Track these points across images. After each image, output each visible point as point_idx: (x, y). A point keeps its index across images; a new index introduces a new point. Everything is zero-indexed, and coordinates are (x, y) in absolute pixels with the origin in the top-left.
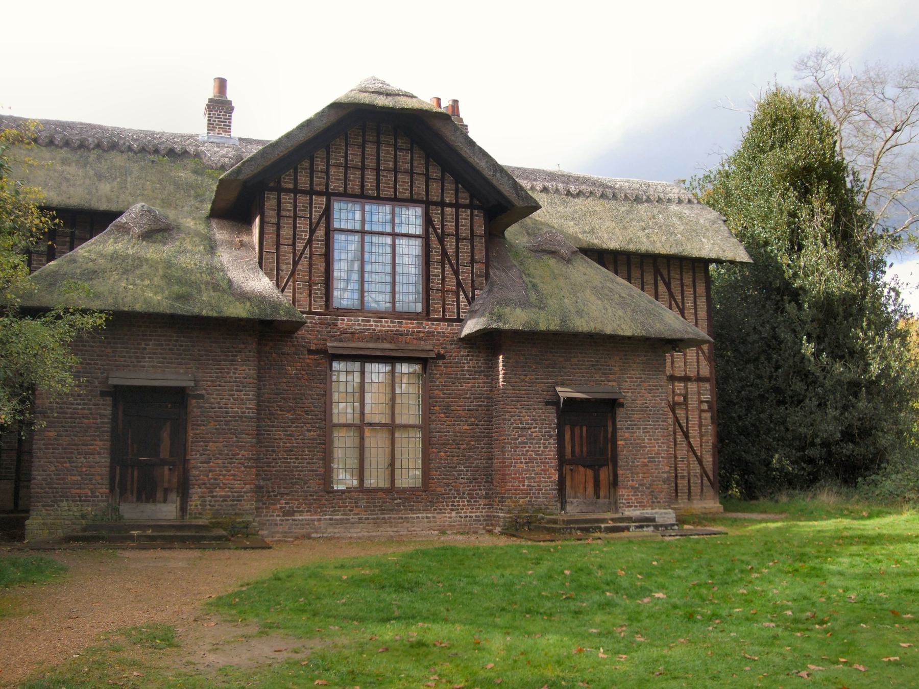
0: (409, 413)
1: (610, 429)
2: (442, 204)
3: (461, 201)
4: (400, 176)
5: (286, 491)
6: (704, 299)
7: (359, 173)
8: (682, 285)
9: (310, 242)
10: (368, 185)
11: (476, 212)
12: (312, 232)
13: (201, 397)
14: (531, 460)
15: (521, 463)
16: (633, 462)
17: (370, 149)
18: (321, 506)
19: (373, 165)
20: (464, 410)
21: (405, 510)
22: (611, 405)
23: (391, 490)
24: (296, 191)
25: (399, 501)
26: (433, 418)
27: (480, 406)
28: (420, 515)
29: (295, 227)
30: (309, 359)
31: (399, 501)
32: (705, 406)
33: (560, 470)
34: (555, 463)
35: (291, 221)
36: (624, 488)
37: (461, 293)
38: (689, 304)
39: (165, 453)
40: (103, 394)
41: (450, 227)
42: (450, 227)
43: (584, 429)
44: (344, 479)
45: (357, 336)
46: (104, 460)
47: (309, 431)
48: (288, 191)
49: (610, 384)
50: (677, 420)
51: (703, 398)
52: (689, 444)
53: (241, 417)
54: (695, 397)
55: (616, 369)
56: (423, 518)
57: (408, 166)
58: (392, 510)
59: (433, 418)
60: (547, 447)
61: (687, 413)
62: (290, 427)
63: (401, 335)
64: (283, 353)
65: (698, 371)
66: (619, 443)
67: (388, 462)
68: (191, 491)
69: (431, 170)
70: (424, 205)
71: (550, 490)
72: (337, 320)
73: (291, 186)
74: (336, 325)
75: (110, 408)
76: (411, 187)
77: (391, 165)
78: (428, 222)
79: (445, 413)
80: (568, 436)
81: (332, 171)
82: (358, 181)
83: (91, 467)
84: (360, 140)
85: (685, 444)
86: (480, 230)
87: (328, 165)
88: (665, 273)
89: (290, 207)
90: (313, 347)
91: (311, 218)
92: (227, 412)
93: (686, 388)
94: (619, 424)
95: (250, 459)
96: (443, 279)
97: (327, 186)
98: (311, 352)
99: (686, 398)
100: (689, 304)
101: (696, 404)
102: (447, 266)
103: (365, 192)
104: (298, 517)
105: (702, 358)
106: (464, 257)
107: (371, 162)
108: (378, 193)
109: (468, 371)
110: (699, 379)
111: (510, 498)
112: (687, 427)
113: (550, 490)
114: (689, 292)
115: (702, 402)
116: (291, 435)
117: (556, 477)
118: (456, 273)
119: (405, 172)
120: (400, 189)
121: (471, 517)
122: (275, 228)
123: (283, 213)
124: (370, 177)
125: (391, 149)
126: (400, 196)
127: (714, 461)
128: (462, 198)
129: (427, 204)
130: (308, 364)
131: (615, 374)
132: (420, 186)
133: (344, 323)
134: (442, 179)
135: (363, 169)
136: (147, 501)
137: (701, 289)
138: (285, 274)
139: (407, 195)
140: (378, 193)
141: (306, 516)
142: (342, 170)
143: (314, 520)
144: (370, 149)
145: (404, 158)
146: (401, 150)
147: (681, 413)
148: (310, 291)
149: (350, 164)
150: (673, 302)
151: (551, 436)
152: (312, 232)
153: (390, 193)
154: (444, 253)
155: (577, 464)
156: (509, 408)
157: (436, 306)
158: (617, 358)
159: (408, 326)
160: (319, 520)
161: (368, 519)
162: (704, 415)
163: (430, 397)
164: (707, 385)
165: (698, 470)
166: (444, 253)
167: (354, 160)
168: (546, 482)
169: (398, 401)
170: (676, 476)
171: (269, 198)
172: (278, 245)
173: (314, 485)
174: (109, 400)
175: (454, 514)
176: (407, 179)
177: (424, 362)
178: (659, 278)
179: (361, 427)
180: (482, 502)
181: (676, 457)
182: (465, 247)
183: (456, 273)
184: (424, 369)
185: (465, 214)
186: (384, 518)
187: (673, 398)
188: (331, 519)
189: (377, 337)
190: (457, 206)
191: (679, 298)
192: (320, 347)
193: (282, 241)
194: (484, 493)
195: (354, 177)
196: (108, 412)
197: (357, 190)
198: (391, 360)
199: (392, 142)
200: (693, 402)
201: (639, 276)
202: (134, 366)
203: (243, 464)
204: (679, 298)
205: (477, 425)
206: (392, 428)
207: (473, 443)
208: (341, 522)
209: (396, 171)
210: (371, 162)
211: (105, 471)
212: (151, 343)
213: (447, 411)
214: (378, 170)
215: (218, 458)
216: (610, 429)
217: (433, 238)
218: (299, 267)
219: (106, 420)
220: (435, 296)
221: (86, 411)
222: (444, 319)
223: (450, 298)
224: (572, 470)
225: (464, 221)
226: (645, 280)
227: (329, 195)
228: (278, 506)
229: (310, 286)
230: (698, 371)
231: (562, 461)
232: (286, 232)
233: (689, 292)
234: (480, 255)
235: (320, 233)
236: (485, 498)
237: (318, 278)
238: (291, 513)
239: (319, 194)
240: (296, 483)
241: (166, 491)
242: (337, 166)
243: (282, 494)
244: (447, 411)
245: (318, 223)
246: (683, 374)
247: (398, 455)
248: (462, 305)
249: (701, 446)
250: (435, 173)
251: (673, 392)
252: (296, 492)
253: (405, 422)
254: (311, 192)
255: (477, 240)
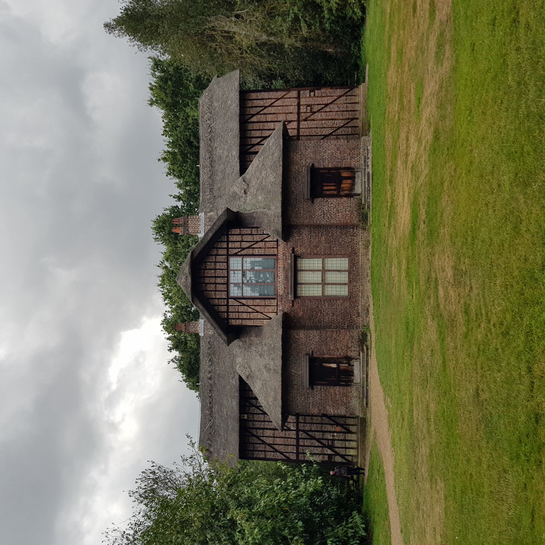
0: (317, 263)
1: (324, 171)
2: (228, 248)
3: (226, 240)
4: (217, 268)
5: (349, 315)
6: (259, 93)
7: (217, 285)
8: (252, 107)
9: (248, 306)
10: (222, 281)
11: (230, 233)
12: (244, 305)
13: (312, 351)
14: (338, 210)
15: (338, 215)
16: (339, 159)
17: (207, 280)
18: (356, 301)
19: (213, 279)
20: (316, 239)
21: (358, 265)
22: (314, 171)
23: (350, 272)
24: (228, 312)
25: (354, 268)
26: (319, 253)
27: (314, 231)
28: (360, 259)
29: (242, 312)
30: (296, 306)
31: (354, 268)
32: (312, 94)
33: (341, 196)
34: (339, 199)
35: (240, 314)
36: (351, 164)
37: (265, 240)
38: (261, 103)
39: (334, 366)
40: (312, 389)
41: (237, 245)
42: (237, 245)
43: (324, 184)
44: (344, 291)
45: (286, 286)
46: (337, 388)
47: (325, 306)
48: (228, 315)
49: (303, 170)
50: (318, 111)
51: (308, 95)
52: (331, 103)
53: (320, 336)
54: (308, 99)
55: (296, 167)
56: (361, 258)
57: (213, 264)
58: (358, 271)
59: (319, 253)
60: (332, 203)
61: (316, 105)
62: (324, 314)
63: (285, 267)
64: (294, 317)
65: (295, 98)
66: (330, 166)
67: (338, 273)
68: (349, 356)
69: (213, 254)
70: (229, 257)
71: (351, 201)
72: (279, 295)
73: (226, 314)
74: (281, 296)
75: (318, 386)
76: (221, 262)
77: (213, 271)
78: (236, 255)
79: (317, 248)
80: (328, 193)
81: (218, 297)
82: (221, 286)
83: (340, 393)
84: (204, 285)
85: (331, 106)
86: (237, 231)
87: (216, 299)
88: (247, 117)
89: (234, 314)
90: (291, 305)
91: (238, 306)
92: (318, 342)
93: (303, 105)
94: (322, 167)
95: (337, 333)
96: (260, 248)
97: (224, 299)
98: (293, 306)
99: (308, 106)
100: (261, 103)
101: (311, 99)
102: (254, 246)
103: (226, 283)
104: (360, 311)
105: (287, 96)
106: (250, 238)
107: (213, 280)
108: (226, 277)
109: (299, 237)
110: (299, 97)
111: (354, 220)
112: (323, 104)
113: (351, 201)
114: (256, 103)
115: (310, 95)
116: (327, 314)
117: (345, 199)
118: (257, 242)
119: (215, 265)
120: (223, 267)
121: (362, 236)
122: (243, 320)
123: (237, 317)
124: (219, 280)
125: (206, 271)
126: (226, 267)
127: (339, 89)
128: (224, 239)
129: (228, 255)
130: (298, 307)
131: (299, 168)
132: (219, 258)
133: (281, 292)
134: (217, 248)
135: (216, 284)
136: (353, 372)
137: (254, 96)
138: (261, 316)
139: (225, 264)
140: (226, 277)
141: (360, 307)
142: (217, 293)
143: (361, 305)
144: (207, 280)
145: (210, 265)
146: (206, 267)
147: (316, 108)
148: (268, 306)
149: (214, 289)
150: (261, 113)
151: (327, 201)
152: (244, 305)
153: (225, 271)
154: (249, 248)
155: (340, 188)
156: (315, 221)
157: (271, 251)
158: (292, 167)
159: (281, 264)
160: (361, 302)
161: (361, 282)
162: (316, 95)
163: (311, 254)
164: (302, 92)
165: (344, 98)
166: (249, 248)
167: (213, 286)
168: (347, 203)
169: (312, 268)
170: (347, 111)
171: (231, 323)
172: (250, 319)
173: (347, 304)
174: (315, 387)
175: (360, 244)
176: (218, 264)
177: (296, 257)
178: (250, 121)
179: (324, 283)
180: (355, 231)
181: (337, 111)
182: (246, 238)
183: (257, 242)
184: (299, 257)
185: (231, 238)
186: (361, 275)
187: (308, 113)
188: (361, 297)
189: (286, 277)
190: (228, 242)
191: (259, 109)
192: (291, 302)
193: (248, 317)
194: (351, 230)
195: (220, 287)
196: (319, 387)
197: (225, 286)
198: (296, 271)
199: (203, 271)
200: (310, 101)
201: (249, 132)
202: (301, 377)
203: (338, 335)
204: (259, 109)
205: (322, 233)
206: (324, 271)
207: (330, 235)
208: (362, 293)
209: (215, 269)
210: (213, 280)
211: (341, 388)
212: (292, 371)
213: (316, 247)
214: (215, 277)
215: (336, 346)
216: (324, 171)
217: (243, 252)
218: (259, 310)
219: (322, 388)
220: (268, 252)
221: (319, 395)
222: (277, 248)
223: (268, 245)
224: (342, 191)
225: (234, 238)
226: (251, 129)
227: (228, 298)
228: (356, 319)
229: (266, 306)
230: (295, 98)
231: (338, 196)
232: (245, 316)
233: (256, 103)
234: (248, 231)
235: (244, 301)
236: (354, 229)
237: (262, 302)
238: (358, 313)
239: (228, 302)
240: (346, 312)
241: (350, 365)
242: (215, 295)
243: (351, 317)
244: (316, 247)
245: (240, 303)
246: (296, 107)
247: (335, 269)
248: (271, 239)
249: (332, 96)
250: (215, 252)
251: (305, 113)
252: (350, 311)
253: (321, 265)
254: (228, 305)
255: (242, 233)
